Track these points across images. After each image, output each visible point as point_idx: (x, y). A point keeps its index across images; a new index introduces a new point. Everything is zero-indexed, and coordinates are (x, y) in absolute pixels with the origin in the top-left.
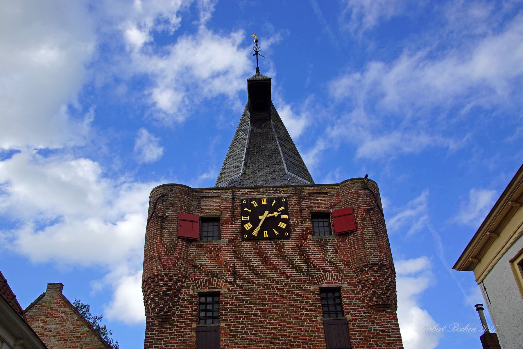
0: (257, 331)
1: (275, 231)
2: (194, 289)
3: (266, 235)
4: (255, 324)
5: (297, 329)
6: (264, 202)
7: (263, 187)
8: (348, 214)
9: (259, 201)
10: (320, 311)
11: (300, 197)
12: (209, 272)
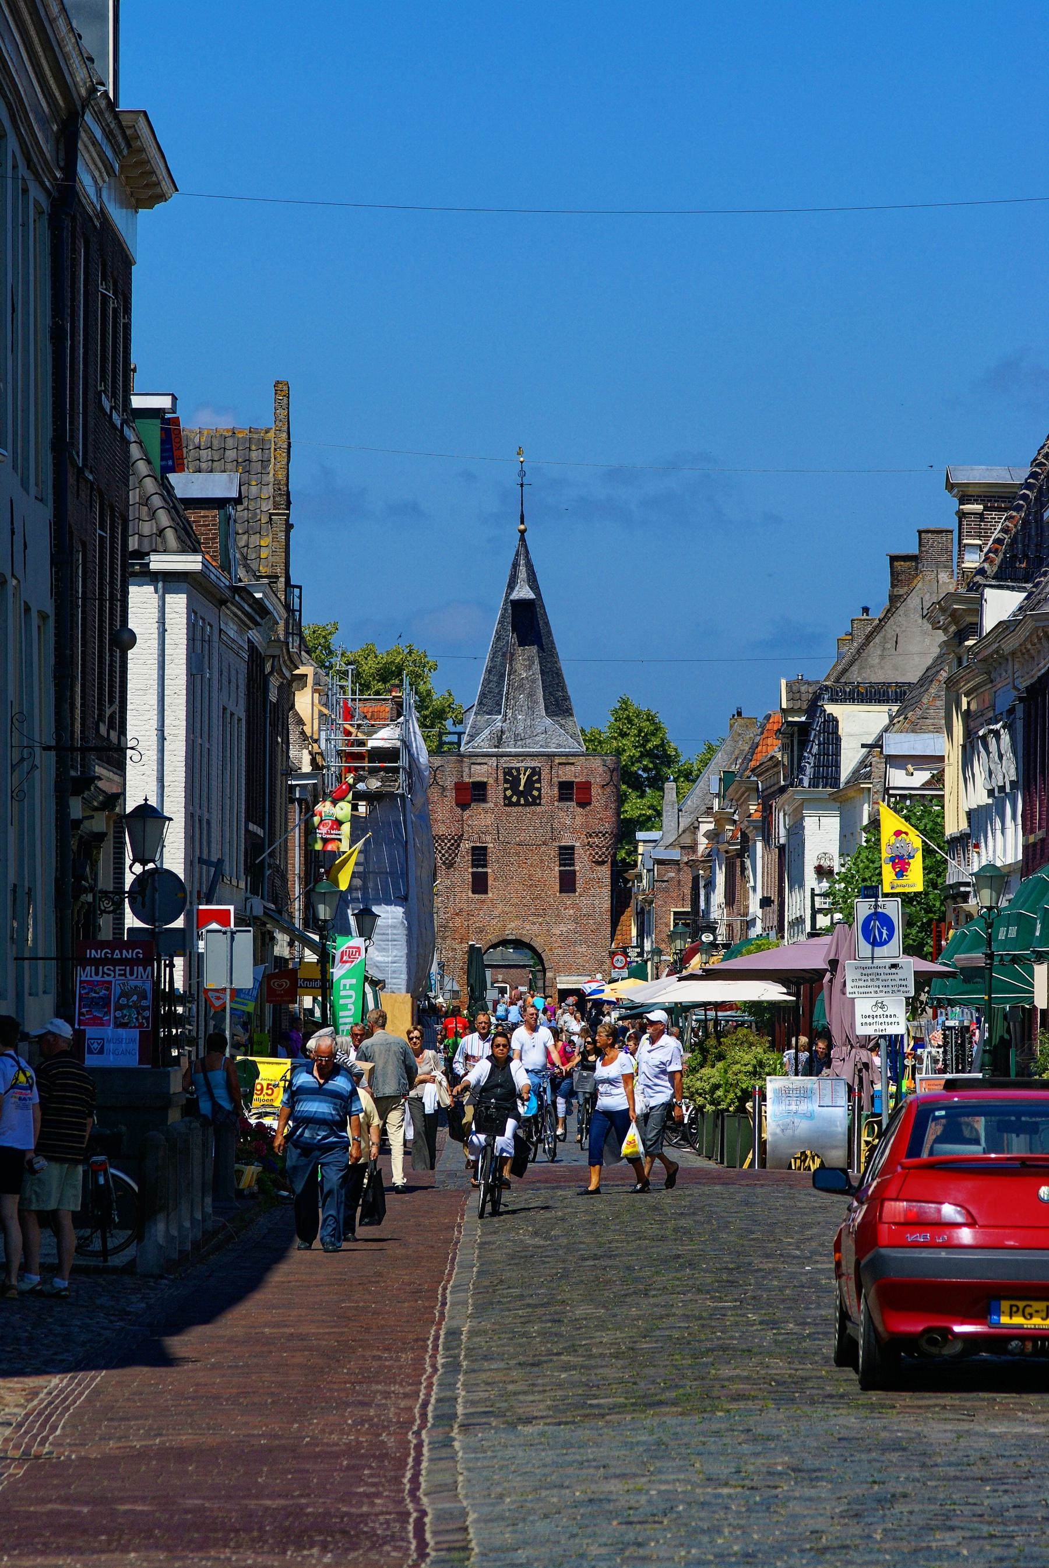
3: (522, 802)
8: (586, 787)
9: (518, 769)
10: (557, 863)
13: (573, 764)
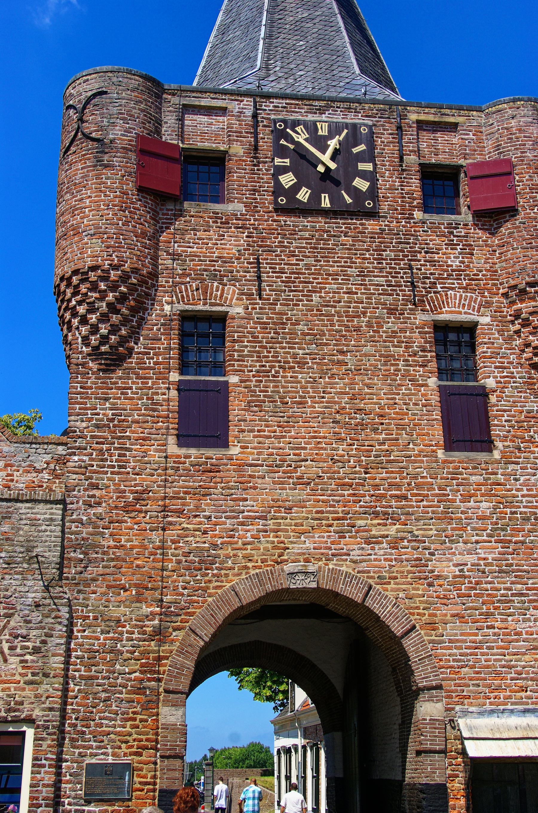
0: (305, 397)
1: (346, 197)
2: (172, 303)
4: (300, 382)
5: (388, 399)
6: (323, 131)
7: (319, 99)
10: (433, 365)
11: (399, 128)
12: (205, 270)
13: (453, 127)
